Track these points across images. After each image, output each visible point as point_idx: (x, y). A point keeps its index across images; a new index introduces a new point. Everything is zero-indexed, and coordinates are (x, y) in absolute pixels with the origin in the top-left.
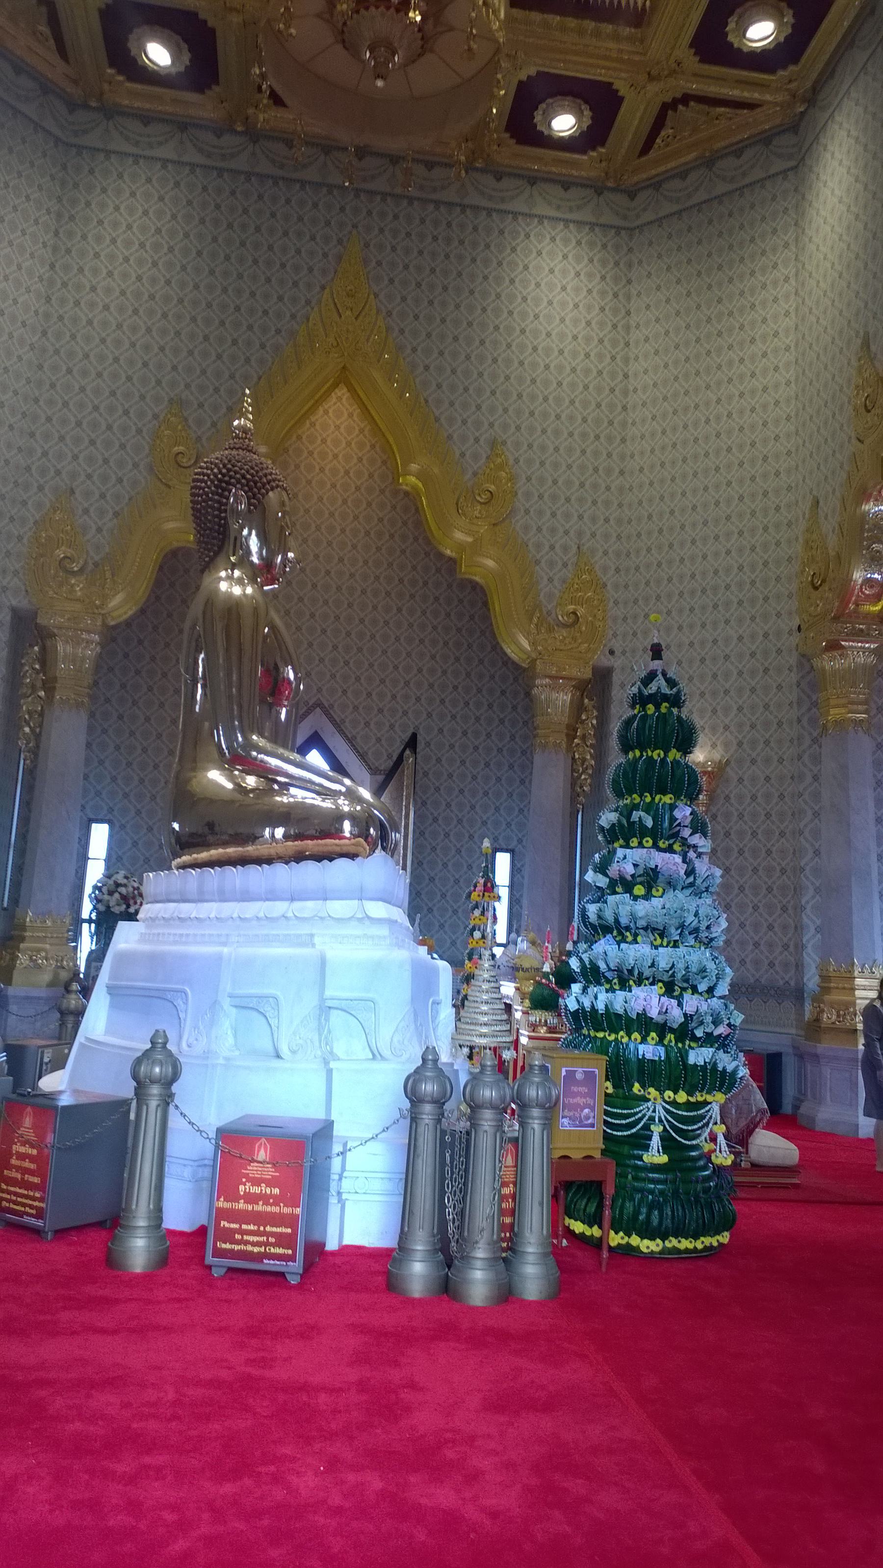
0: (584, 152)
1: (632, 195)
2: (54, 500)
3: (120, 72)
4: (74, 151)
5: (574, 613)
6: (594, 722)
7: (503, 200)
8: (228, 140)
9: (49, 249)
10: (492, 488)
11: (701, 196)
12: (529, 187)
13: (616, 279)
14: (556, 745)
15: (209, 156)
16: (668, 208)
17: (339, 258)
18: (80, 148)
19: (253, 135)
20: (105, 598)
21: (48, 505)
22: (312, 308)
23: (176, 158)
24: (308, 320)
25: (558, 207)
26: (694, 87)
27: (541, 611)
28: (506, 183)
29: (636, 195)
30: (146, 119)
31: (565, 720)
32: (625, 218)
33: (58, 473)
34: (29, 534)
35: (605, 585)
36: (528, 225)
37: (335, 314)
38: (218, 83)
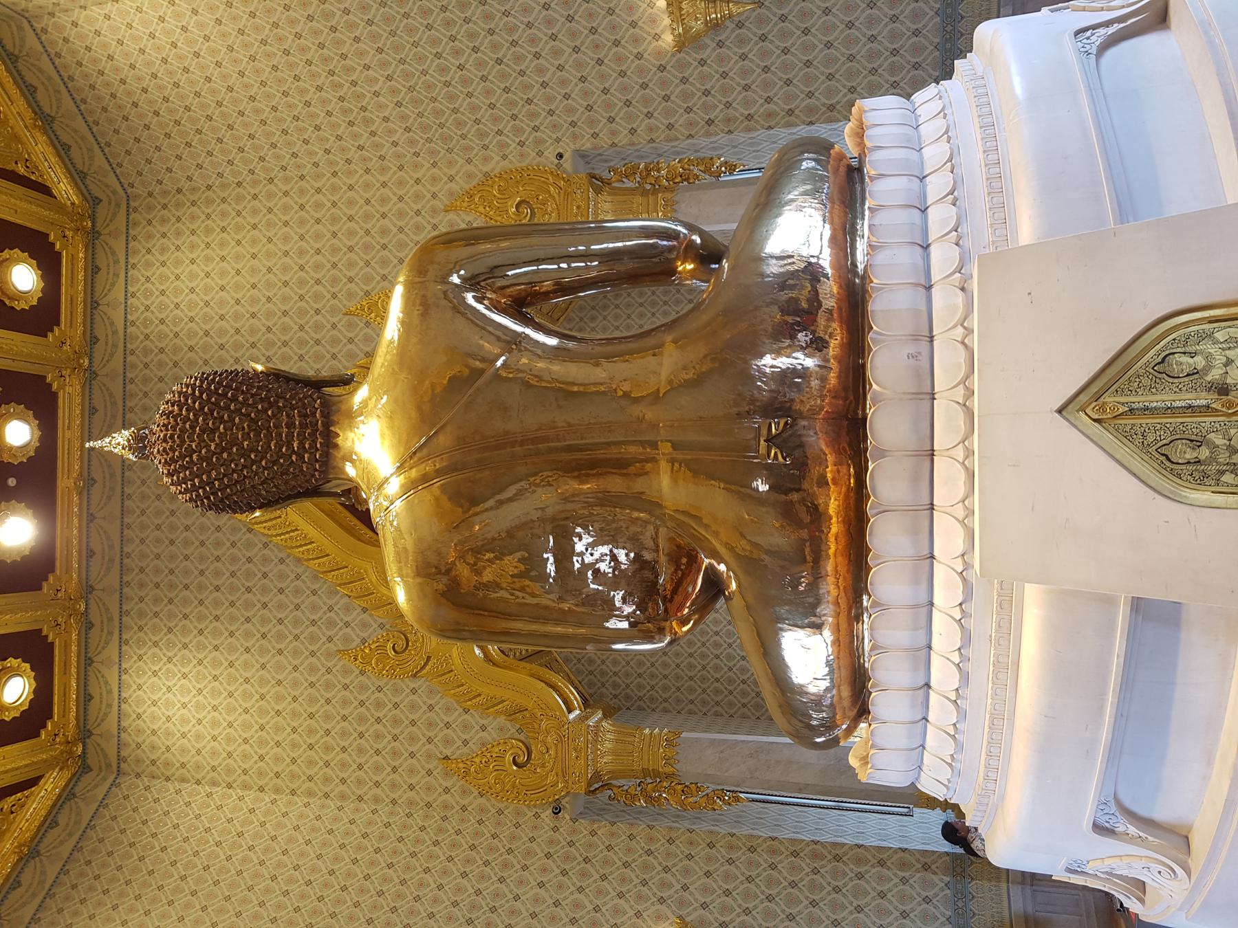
0: (59, 254)
1: (96, 201)
2: (456, 777)
4: (123, 765)
7: (115, 333)
9: (214, 790)
11: (79, 123)
12: (100, 307)
13: (179, 205)
15: (110, 633)
16: (100, 161)
18: (123, 760)
21: (462, 782)
23: (117, 666)
25: (116, 275)
28: (99, 332)
29: (96, 198)
30: (86, 698)
32: (118, 205)
33: (429, 773)
34: (493, 801)
35: (486, 174)
36: (137, 309)
38: (40, 630)
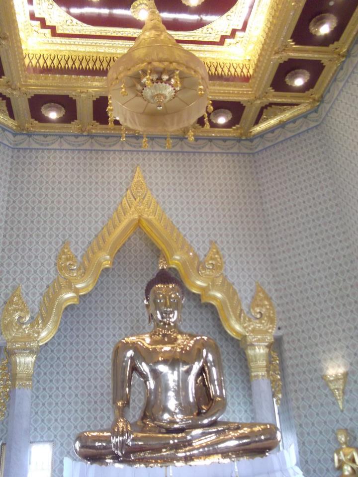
3: (36, 120)
5: (260, 312)
6: (278, 362)
8: (80, 139)
10: (214, 263)
14: (263, 376)
17: (133, 177)
19: (92, 136)
20: (39, 333)
22: (123, 198)
24: (122, 203)
26: (272, 100)
27: (244, 314)
31: (264, 363)
35: (271, 298)
37: (134, 199)
